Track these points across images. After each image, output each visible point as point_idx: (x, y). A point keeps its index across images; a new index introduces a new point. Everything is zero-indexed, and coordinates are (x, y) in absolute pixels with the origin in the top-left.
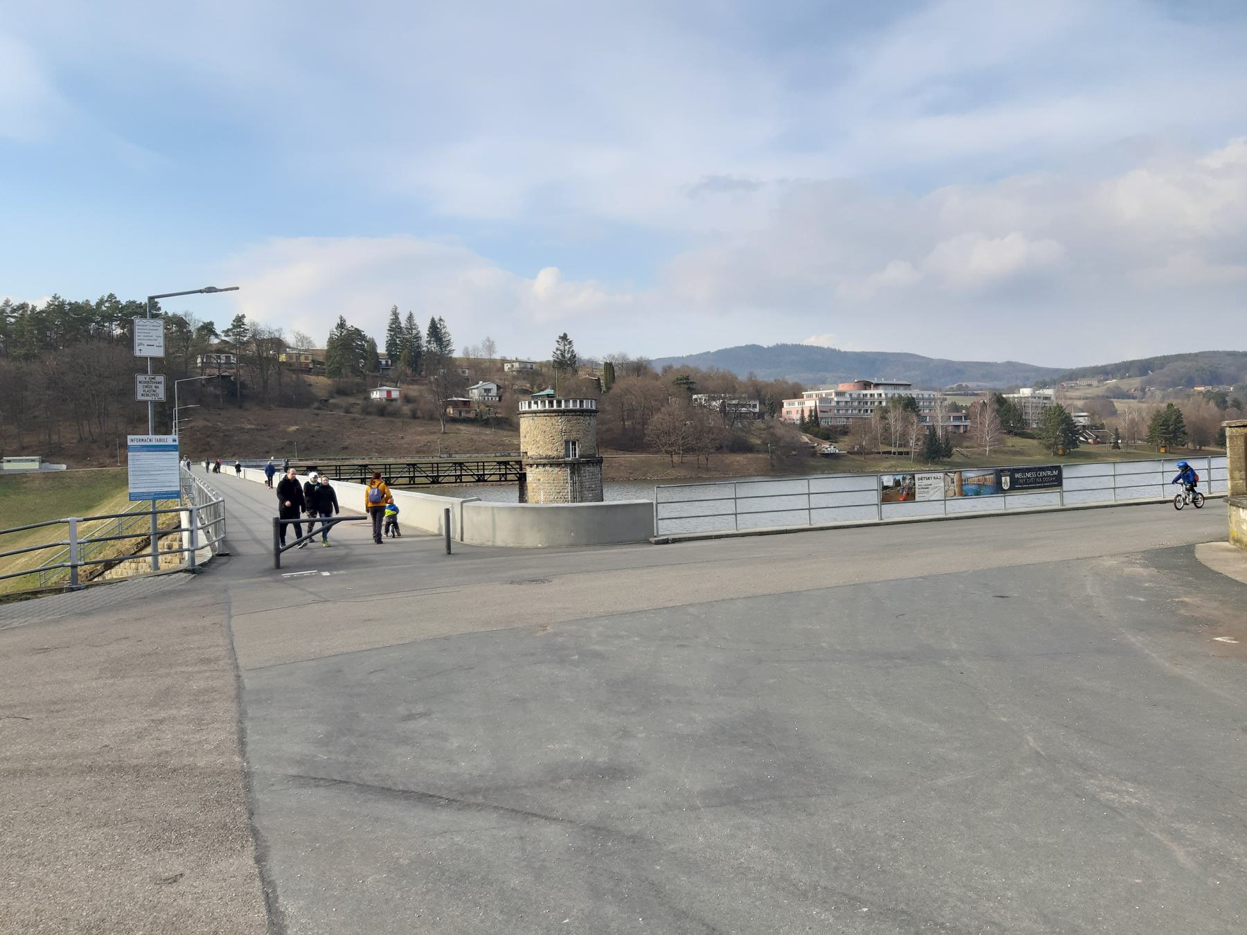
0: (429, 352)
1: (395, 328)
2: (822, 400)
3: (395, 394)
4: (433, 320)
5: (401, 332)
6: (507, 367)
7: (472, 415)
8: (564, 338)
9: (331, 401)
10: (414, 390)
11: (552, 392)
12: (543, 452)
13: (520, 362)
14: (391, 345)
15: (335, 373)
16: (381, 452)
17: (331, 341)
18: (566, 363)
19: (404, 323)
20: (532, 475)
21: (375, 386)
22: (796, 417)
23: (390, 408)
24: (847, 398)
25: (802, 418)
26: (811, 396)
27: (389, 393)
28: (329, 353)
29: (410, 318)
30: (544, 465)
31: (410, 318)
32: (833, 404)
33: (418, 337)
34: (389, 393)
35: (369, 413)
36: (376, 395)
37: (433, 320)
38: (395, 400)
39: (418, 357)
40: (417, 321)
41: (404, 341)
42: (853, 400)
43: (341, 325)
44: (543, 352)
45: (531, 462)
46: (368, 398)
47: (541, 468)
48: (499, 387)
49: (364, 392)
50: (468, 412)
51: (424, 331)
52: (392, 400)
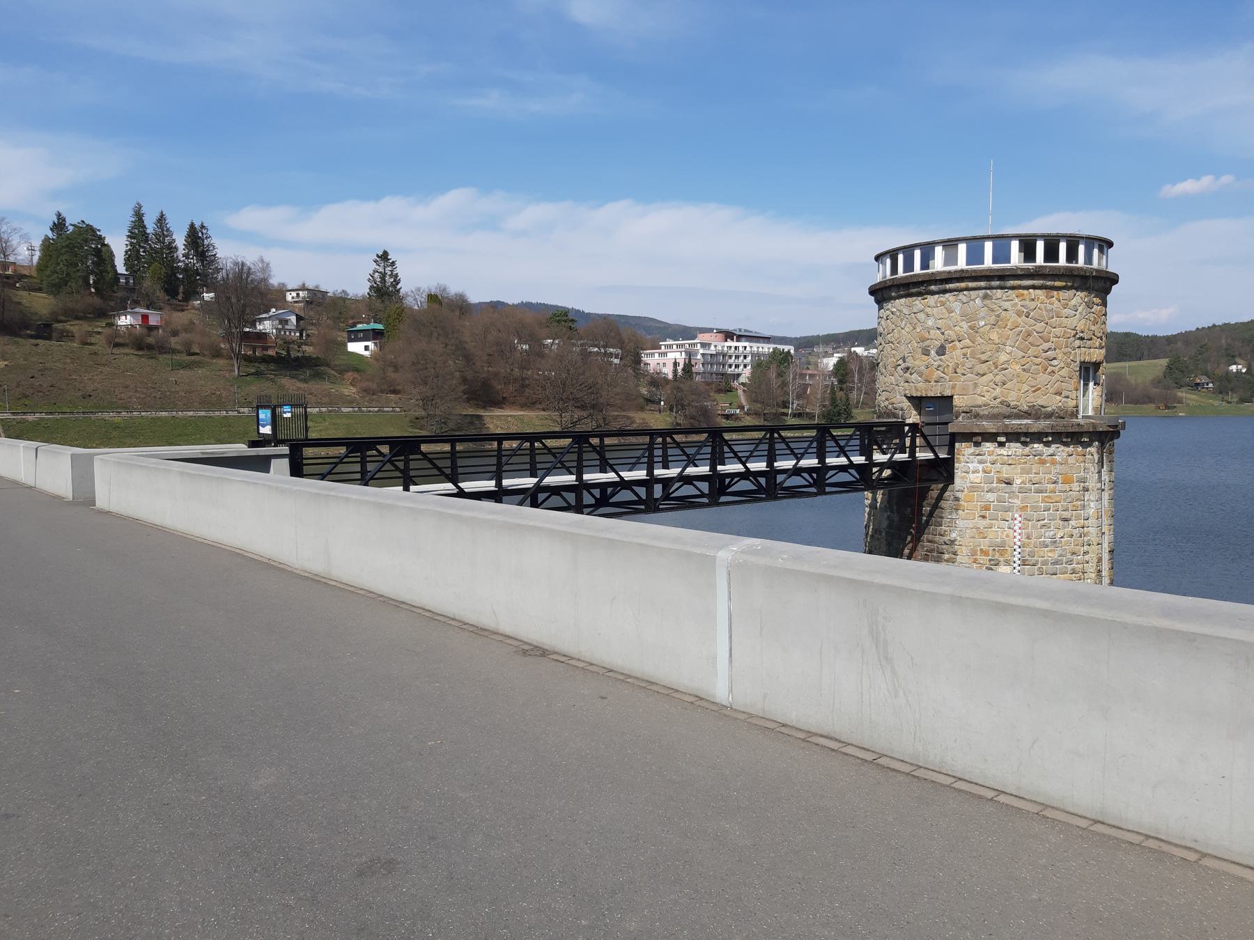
0: (186, 270)
1: (137, 232)
2: (690, 355)
3: (154, 320)
4: (192, 226)
5: (146, 241)
6: (289, 297)
7: (271, 352)
8: (384, 256)
9: (59, 326)
10: (180, 318)
11: (380, 327)
12: (1020, 396)
13: (308, 290)
14: (131, 257)
15: (56, 288)
16: (146, 407)
17: (47, 245)
18: (385, 291)
19: (151, 227)
20: (972, 466)
21: (122, 308)
22: (668, 371)
23: (151, 340)
24: (712, 350)
25: (675, 371)
26: (670, 346)
27: (145, 318)
28: (41, 267)
29: (161, 220)
30: (1038, 437)
31: (161, 220)
32: (699, 357)
33: (172, 248)
34: (145, 318)
35: (117, 345)
36: (125, 321)
37: (192, 226)
38: (156, 328)
39: (175, 271)
40: (171, 223)
41: (155, 255)
42: (717, 354)
43: (59, 225)
44: (352, 280)
45: (989, 426)
46: (111, 325)
47: (1014, 448)
48: (299, 318)
49: (104, 314)
50: (266, 348)
51: (180, 240)
52: (151, 329)
